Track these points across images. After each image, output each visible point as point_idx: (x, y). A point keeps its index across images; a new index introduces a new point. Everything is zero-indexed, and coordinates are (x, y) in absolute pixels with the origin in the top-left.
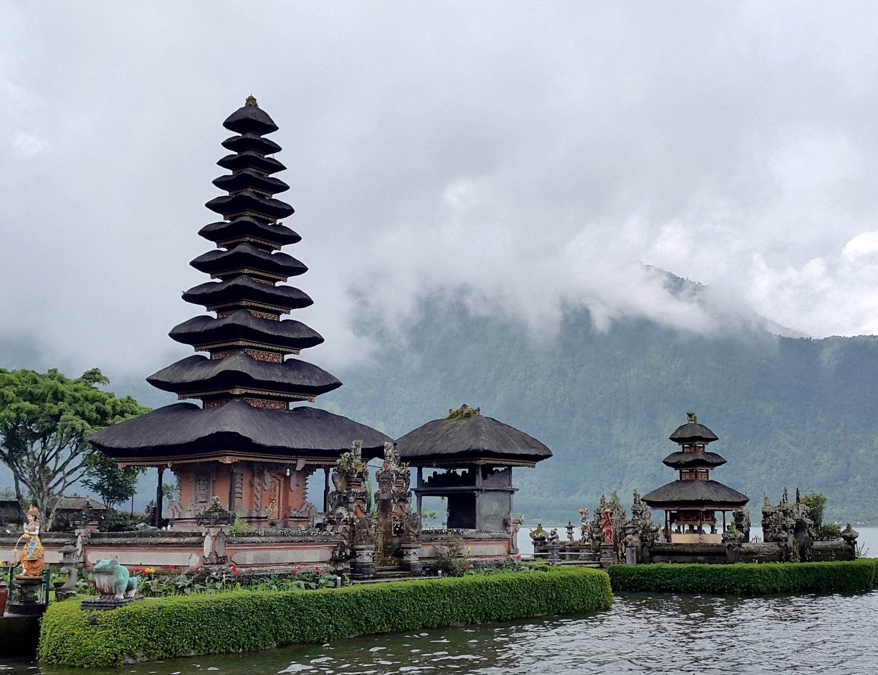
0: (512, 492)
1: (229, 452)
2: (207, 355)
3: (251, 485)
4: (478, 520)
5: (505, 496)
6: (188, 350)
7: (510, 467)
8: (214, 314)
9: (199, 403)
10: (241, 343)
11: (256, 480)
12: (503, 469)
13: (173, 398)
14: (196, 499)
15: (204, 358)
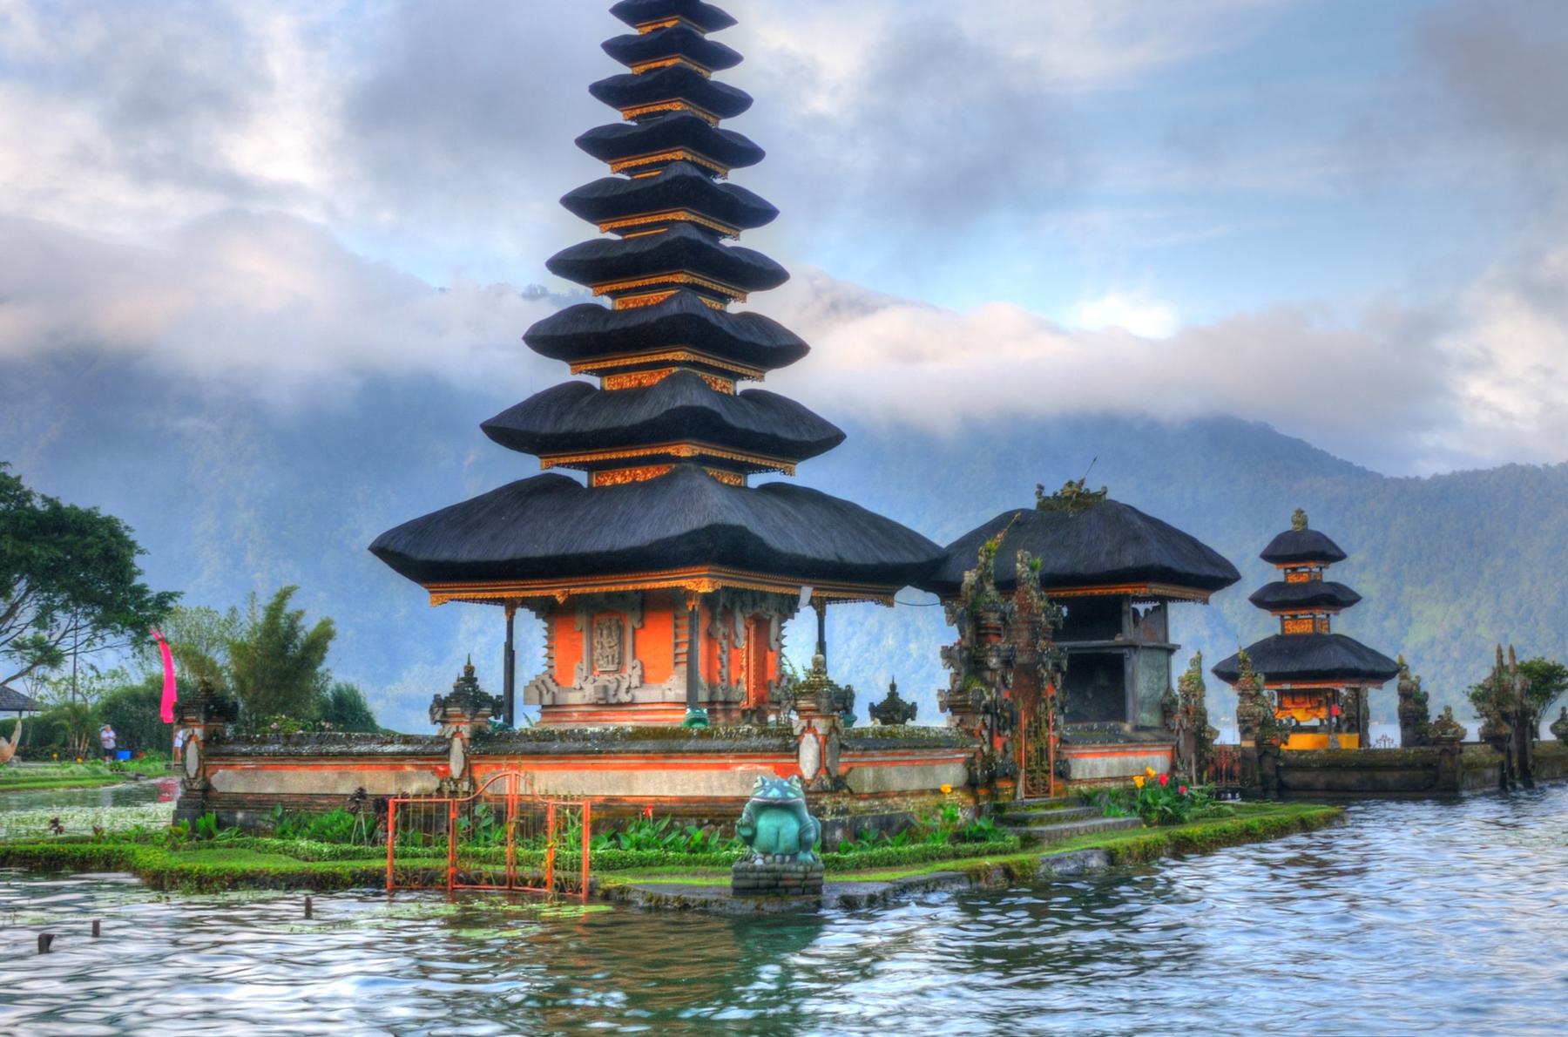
0: (1171, 650)
1: (704, 570)
2: (596, 382)
3: (710, 636)
4: (1130, 705)
5: (1161, 657)
6: (558, 373)
7: (1163, 600)
8: (607, 302)
9: (581, 477)
10: (681, 356)
11: (721, 629)
12: (1150, 606)
13: (529, 466)
14: (592, 668)
15: (588, 388)
